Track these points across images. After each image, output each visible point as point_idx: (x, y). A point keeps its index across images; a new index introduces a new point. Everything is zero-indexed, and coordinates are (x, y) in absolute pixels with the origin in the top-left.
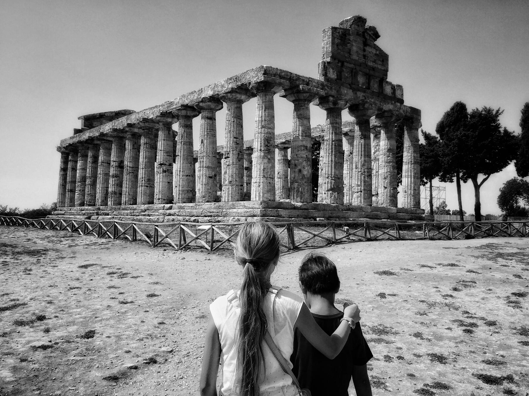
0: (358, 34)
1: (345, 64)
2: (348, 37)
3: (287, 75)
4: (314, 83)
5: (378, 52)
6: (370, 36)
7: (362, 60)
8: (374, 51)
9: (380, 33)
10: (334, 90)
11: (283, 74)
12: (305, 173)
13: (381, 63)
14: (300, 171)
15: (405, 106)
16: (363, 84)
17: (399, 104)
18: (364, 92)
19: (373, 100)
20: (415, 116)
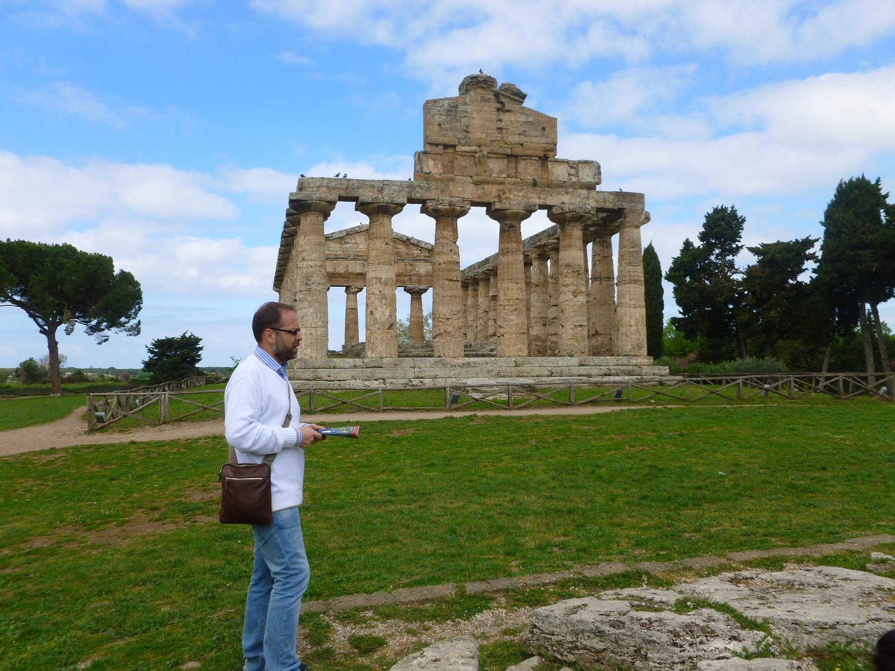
0: (484, 100)
1: (459, 148)
2: (461, 108)
3: (341, 184)
4: (393, 187)
5: (530, 119)
6: (509, 97)
7: (497, 136)
8: (523, 119)
9: (524, 90)
11: (333, 184)
12: (378, 316)
13: (538, 133)
14: (372, 313)
15: (598, 192)
16: (501, 172)
17: (584, 192)
18: (502, 183)
19: (521, 194)
20: (625, 205)
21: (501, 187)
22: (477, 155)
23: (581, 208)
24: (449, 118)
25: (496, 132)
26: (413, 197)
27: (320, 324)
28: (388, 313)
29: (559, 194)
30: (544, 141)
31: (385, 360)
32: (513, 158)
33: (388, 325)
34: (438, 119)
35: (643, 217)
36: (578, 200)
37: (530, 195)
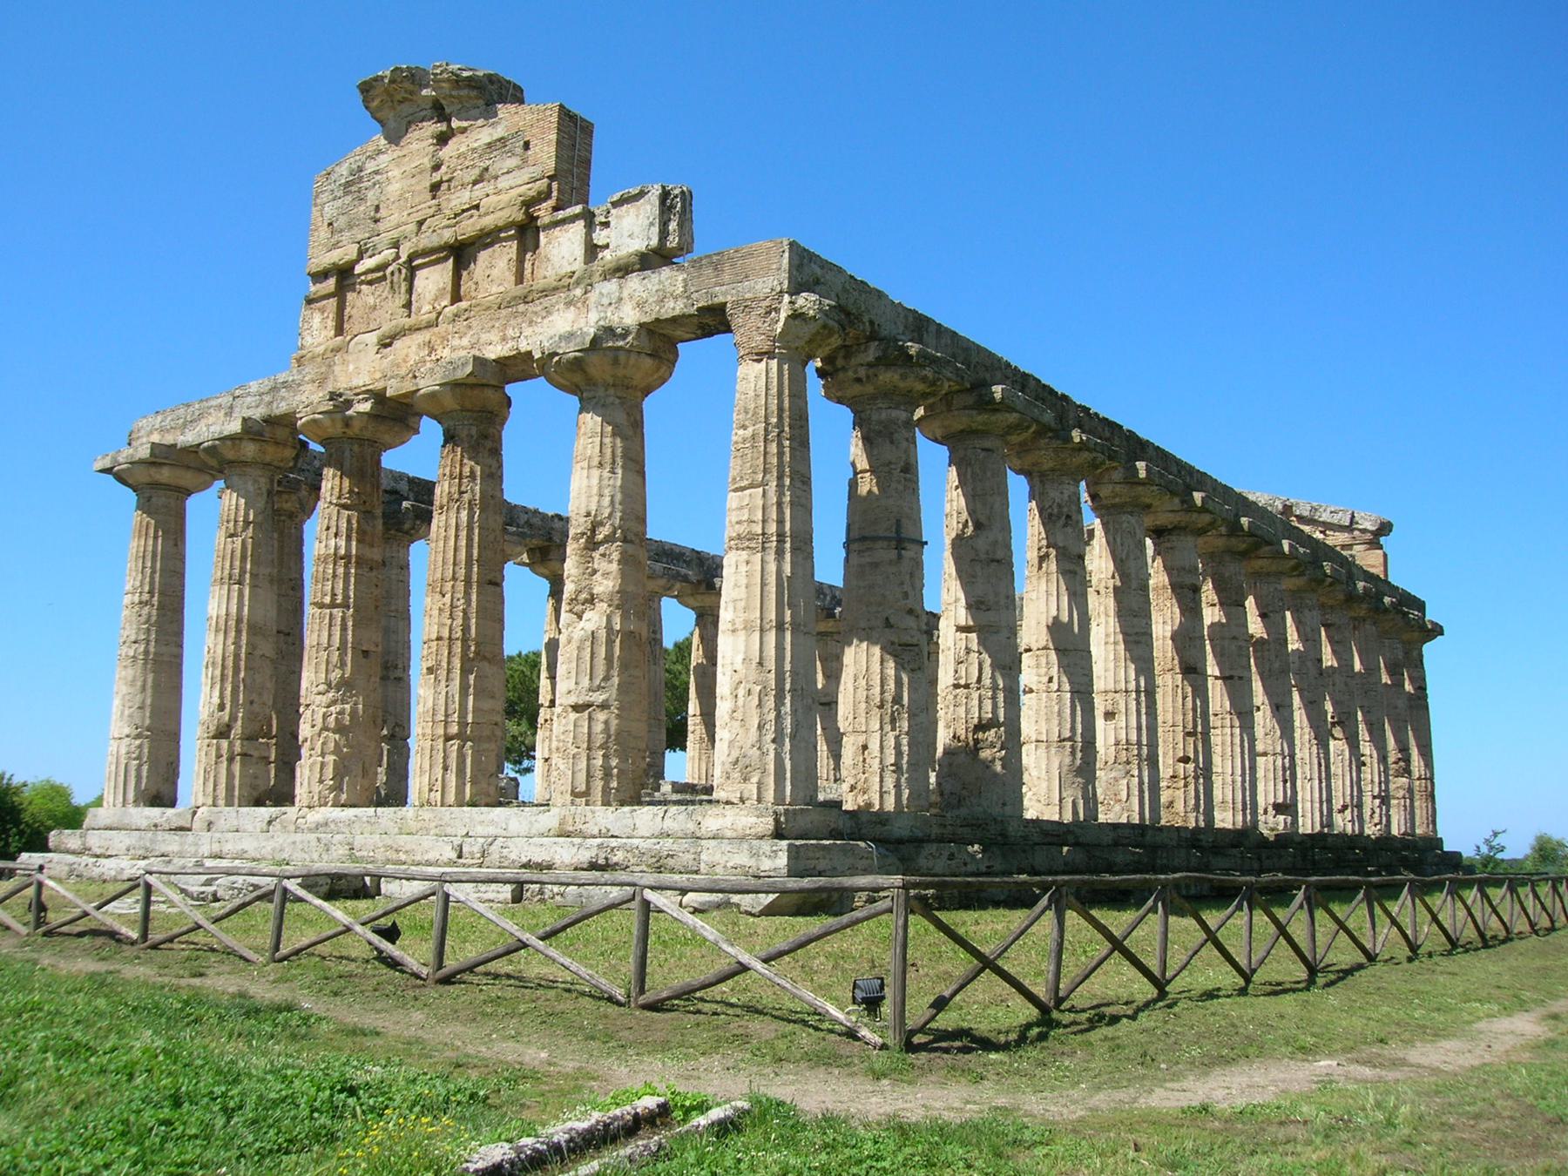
2: (370, 167)
4: (249, 399)
10: (308, 387)
13: (512, 162)
17: (611, 286)
18: (429, 326)
19: (465, 342)
21: (425, 336)
22: (390, 269)
23: (570, 336)
24: (349, 198)
25: (429, 196)
26: (277, 412)
27: (127, 731)
28: (216, 700)
29: (548, 311)
30: (525, 175)
31: (200, 811)
32: (461, 254)
33: (213, 728)
34: (329, 211)
35: (783, 315)
36: (593, 316)
37: (484, 337)
